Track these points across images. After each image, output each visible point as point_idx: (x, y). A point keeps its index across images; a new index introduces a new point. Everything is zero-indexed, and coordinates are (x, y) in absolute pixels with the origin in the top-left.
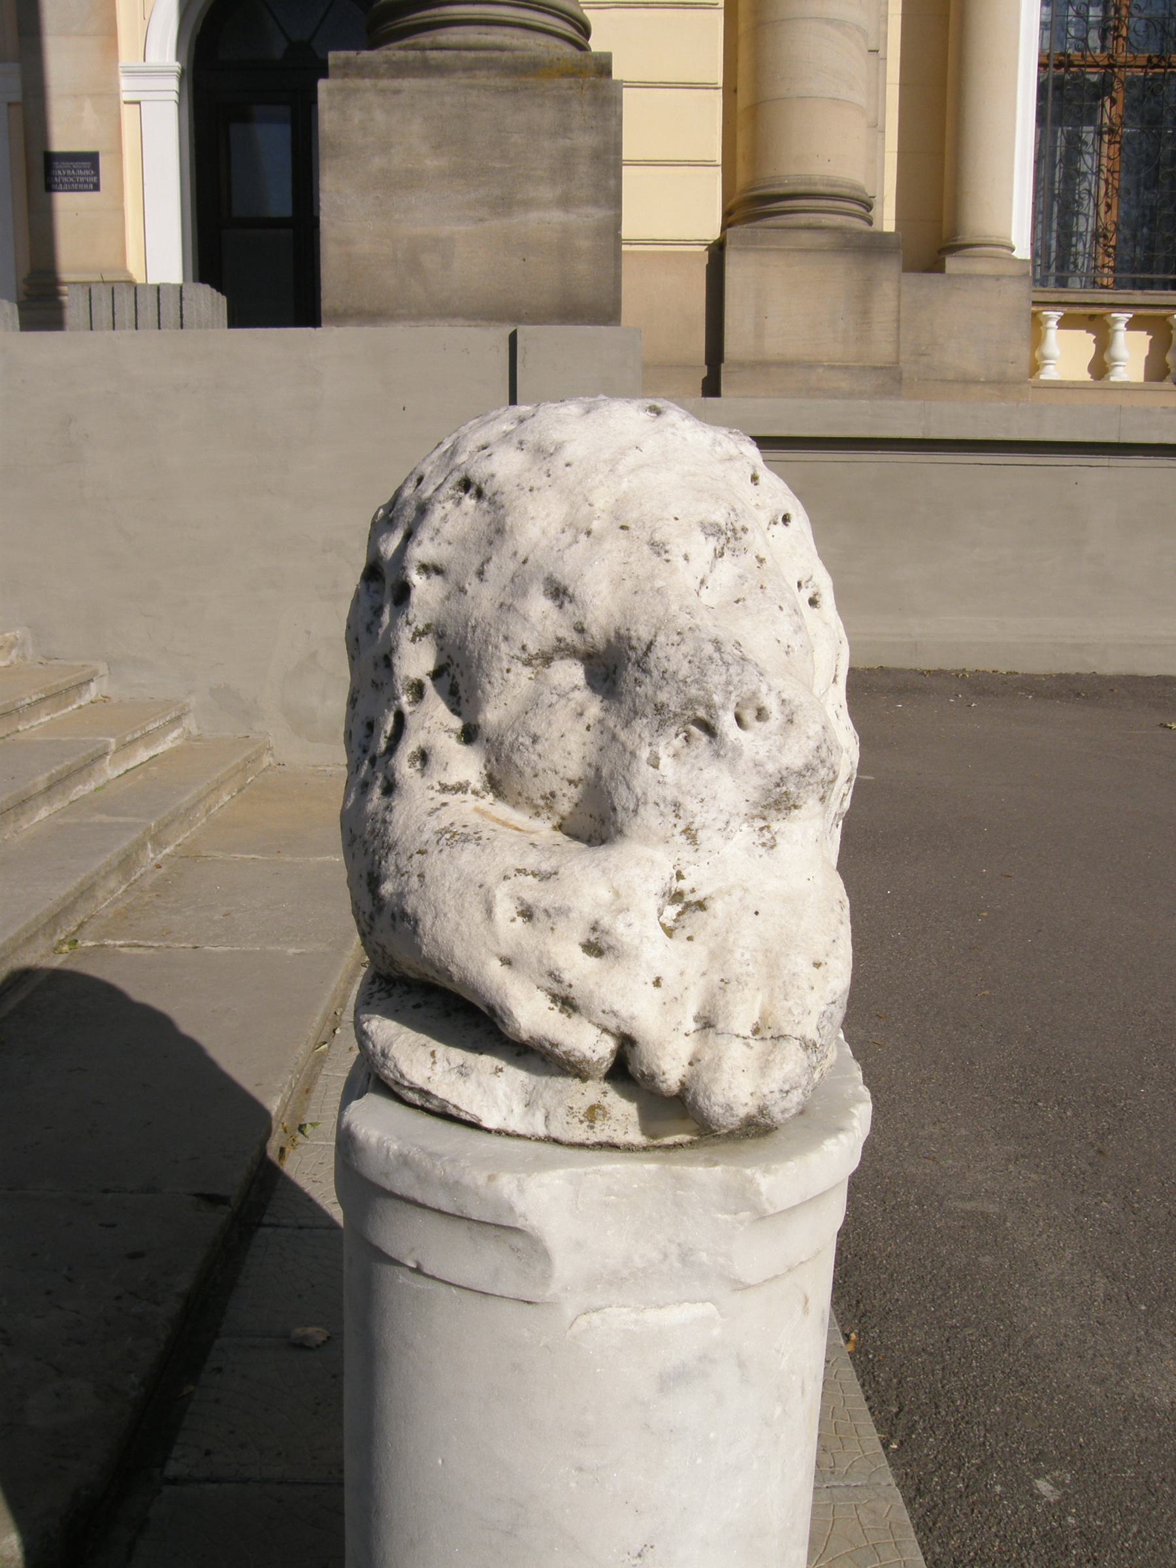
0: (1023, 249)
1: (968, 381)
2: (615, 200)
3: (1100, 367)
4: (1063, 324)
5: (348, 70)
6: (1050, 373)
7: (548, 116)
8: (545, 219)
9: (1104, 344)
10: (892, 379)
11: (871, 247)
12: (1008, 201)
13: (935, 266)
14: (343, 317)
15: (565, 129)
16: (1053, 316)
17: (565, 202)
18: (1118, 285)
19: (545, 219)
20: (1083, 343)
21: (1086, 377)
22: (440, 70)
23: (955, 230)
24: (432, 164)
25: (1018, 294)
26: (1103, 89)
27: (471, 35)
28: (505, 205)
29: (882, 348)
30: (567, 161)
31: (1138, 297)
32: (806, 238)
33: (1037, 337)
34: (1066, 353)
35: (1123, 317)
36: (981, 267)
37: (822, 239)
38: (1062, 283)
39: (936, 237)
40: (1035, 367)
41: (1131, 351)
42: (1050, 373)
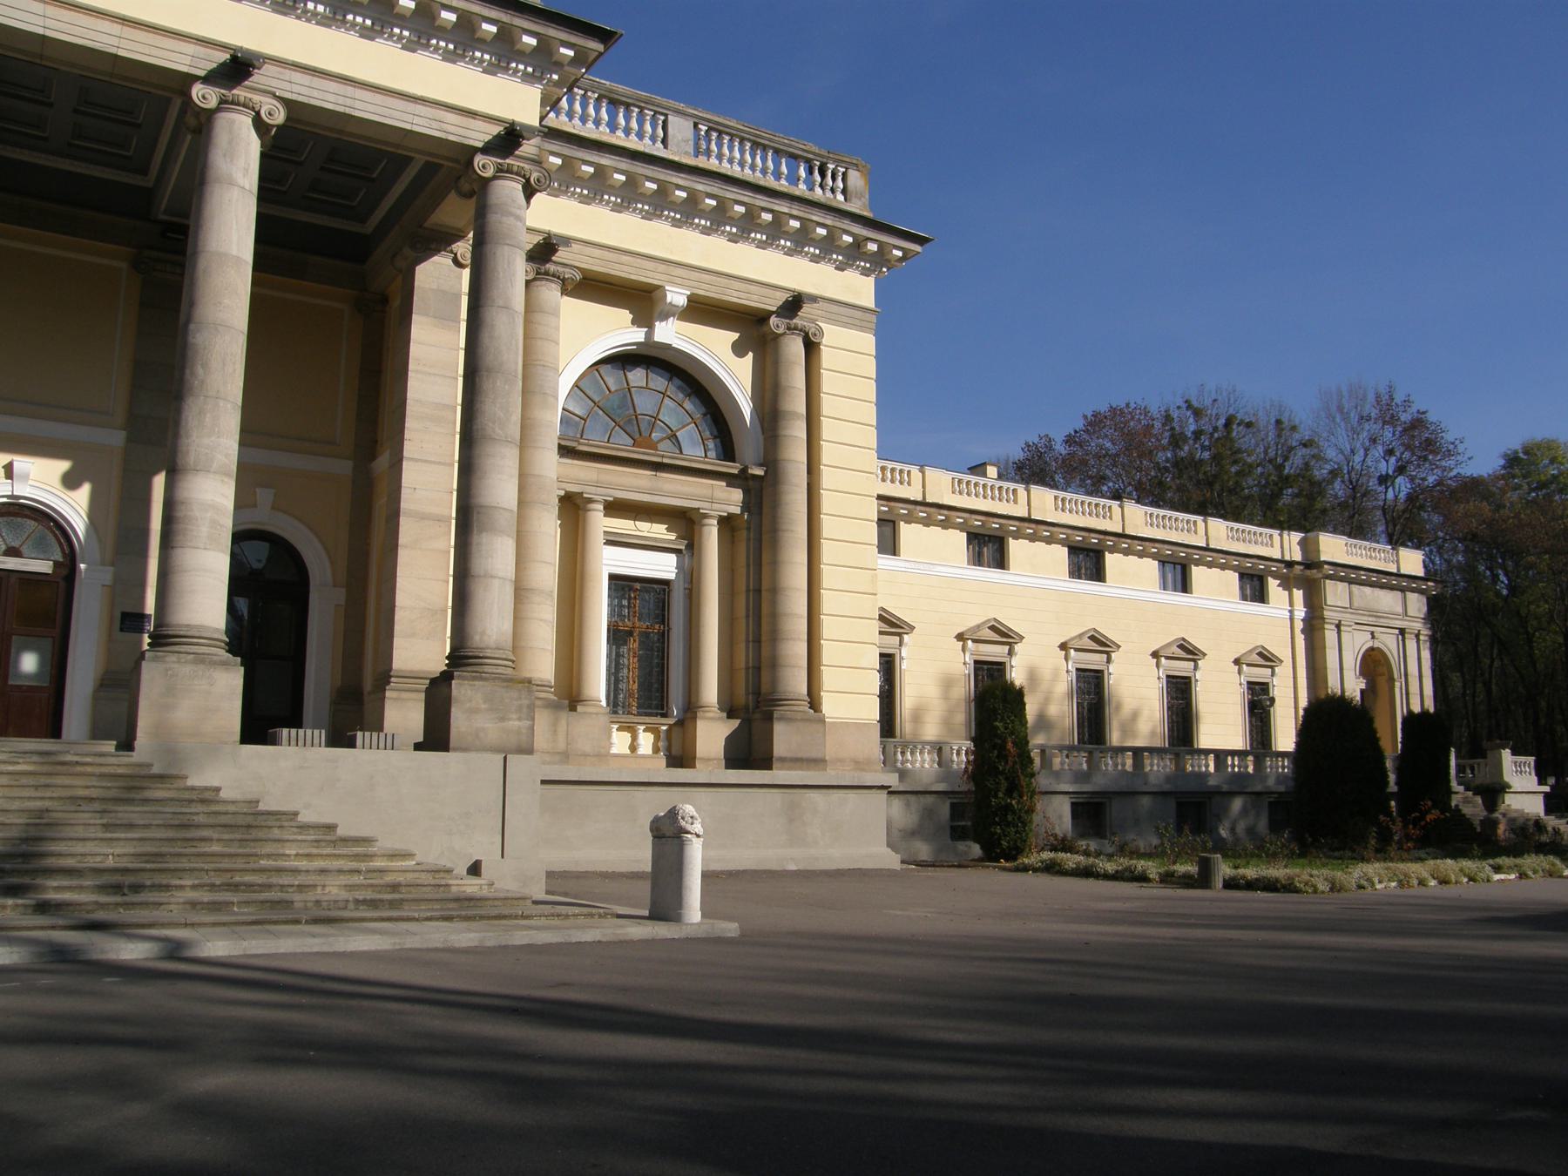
0: (604, 703)
1: (586, 755)
2: (533, 719)
3: (633, 748)
5: (460, 677)
7: (515, 694)
8: (514, 724)
9: (634, 738)
12: (597, 683)
13: (573, 708)
14: (456, 750)
17: (519, 719)
18: (639, 714)
19: (514, 724)
20: (627, 736)
23: (579, 693)
25: (604, 719)
26: (630, 633)
28: (502, 719)
29: (561, 746)
30: (520, 709)
34: (620, 742)
35: (642, 727)
36: (590, 709)
38: (615, 712)
39: (570, 696)
41: (646, 741)
42: (614, 750)
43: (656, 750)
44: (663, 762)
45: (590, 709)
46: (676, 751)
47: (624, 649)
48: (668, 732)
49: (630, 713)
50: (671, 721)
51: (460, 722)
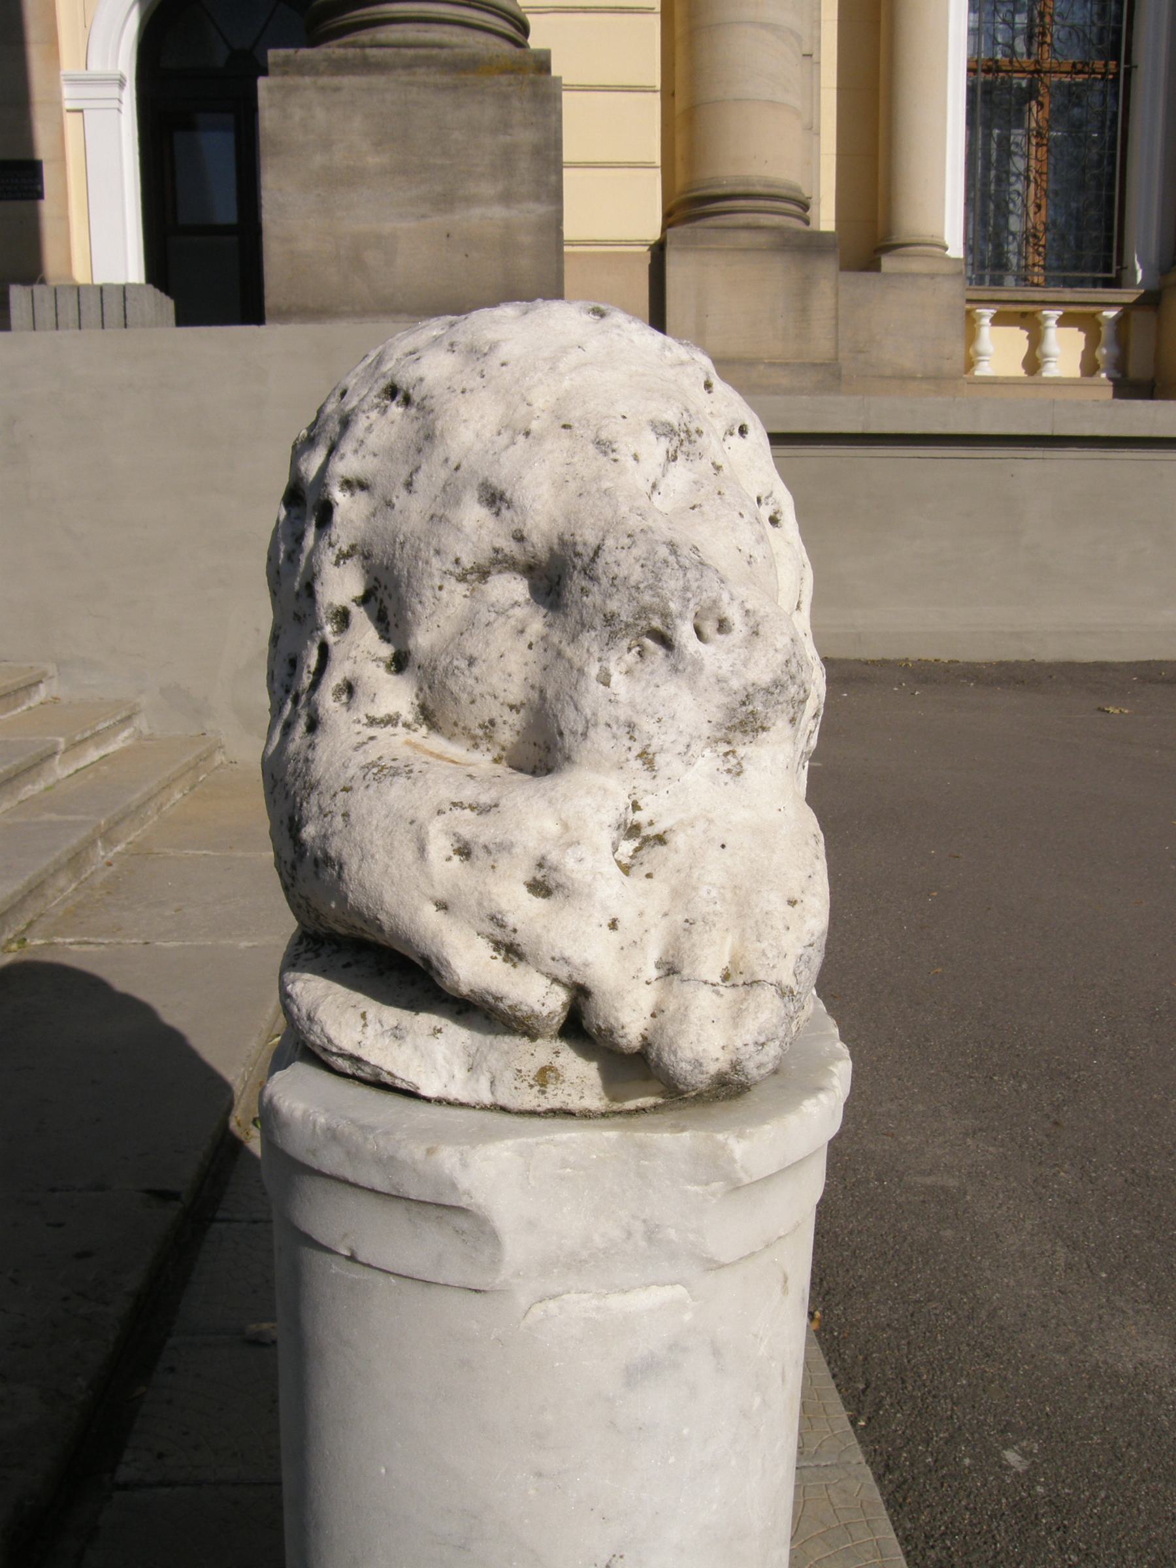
0: (956, 248)
1: (905, 377)
2: (557, 196)
3: (1033, 363)
4: (997, 321)
5: (286, 67)
6: (985, 369)
7: (488, 113)
8: (486, 215)
9: (1036, 340)
10: (831, 375)
11: (810, 245)
12: (940, 203)
13: (870, 264)
14: (286, 315)
15: (505, 126)
16: (986, 314)
17: (507, 198)
18: (1049, 282)
19: (486, 215)
20: (1016, 339)
21: (1021, 372)
22: (380, 67)
23: (889, 232)
24: (373, 161)
25: (953, 291)
26: (1031, 93)
27: (410, 33)
28: (447, 201)
29: (821, 345)
30: (507, 158)
31: (1068, 294)
32: (745, 238)
33: (971, 334)
34: (1000, 350)
35: (1054, 314)
36: (916, 266)
37: (761, 239)
38: (997, 282)
39: (872, 238)
40: (970, 364)
41: (1065, 349)
42: (985, 369)
43: (1089, 367)
44: (1108, 392)
45: (916, 266)
46: (1137, 369)
47: (1017, 136)
48: (1121, 323)
49: (1024, 280)
50: (1128, 296)
51: (294, 220)
